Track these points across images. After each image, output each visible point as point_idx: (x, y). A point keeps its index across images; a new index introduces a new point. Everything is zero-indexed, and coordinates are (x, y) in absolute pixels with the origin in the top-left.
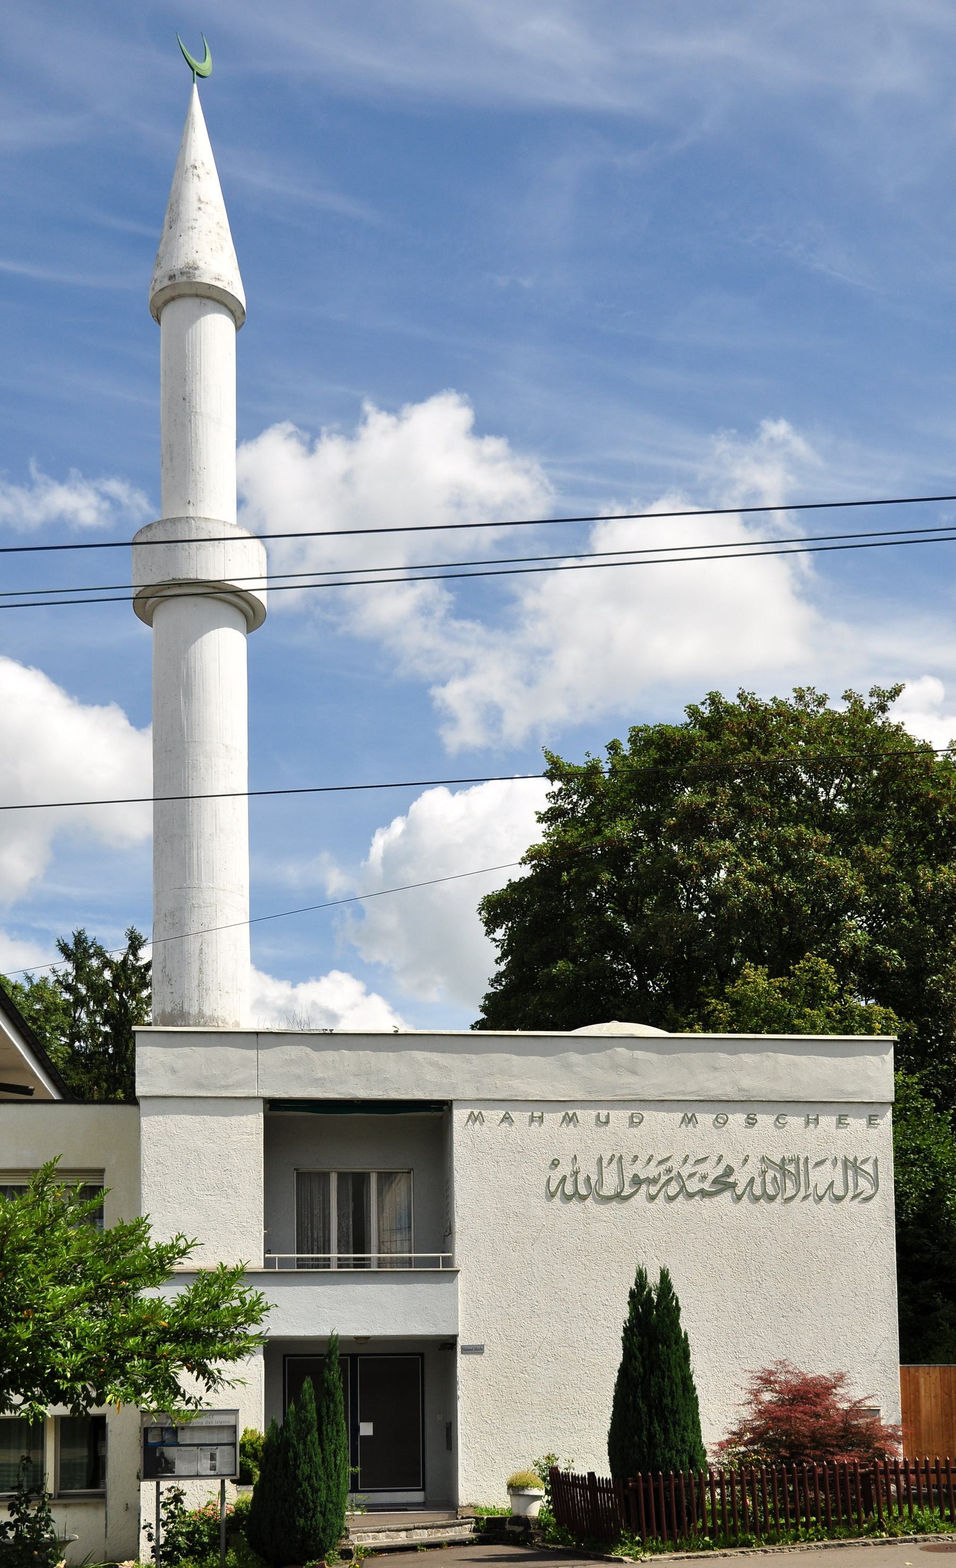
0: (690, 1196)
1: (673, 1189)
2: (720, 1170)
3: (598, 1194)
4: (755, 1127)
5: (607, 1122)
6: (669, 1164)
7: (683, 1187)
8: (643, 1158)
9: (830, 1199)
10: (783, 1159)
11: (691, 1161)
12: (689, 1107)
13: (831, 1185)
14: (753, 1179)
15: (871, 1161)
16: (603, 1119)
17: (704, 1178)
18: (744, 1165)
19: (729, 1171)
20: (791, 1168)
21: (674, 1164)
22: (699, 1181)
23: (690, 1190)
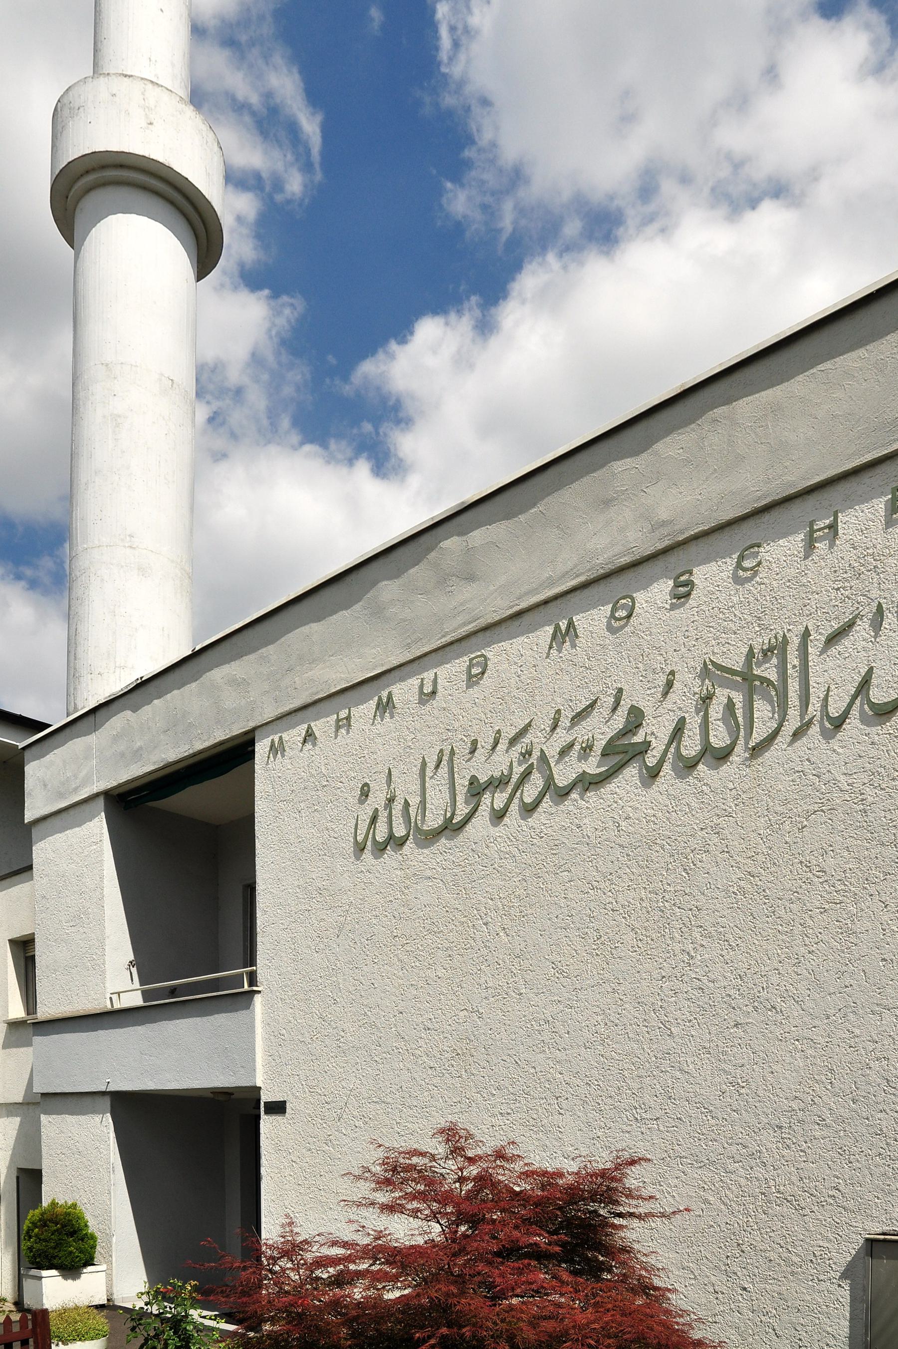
0: (563, 794)
1: (529, 793)
2: (619, 721)
4: (692, 602)
5: (434, 693)
6: (526, 740)
7: (549, 782)
8: (485, 742)
9: (864, 720)
10: (751, 653)
11: (565, 722)
12: (550, 610)
13: (865, 684)
14: (682, 720)
17: (587, 749)
18: (665, 694)
22: (580, 759)
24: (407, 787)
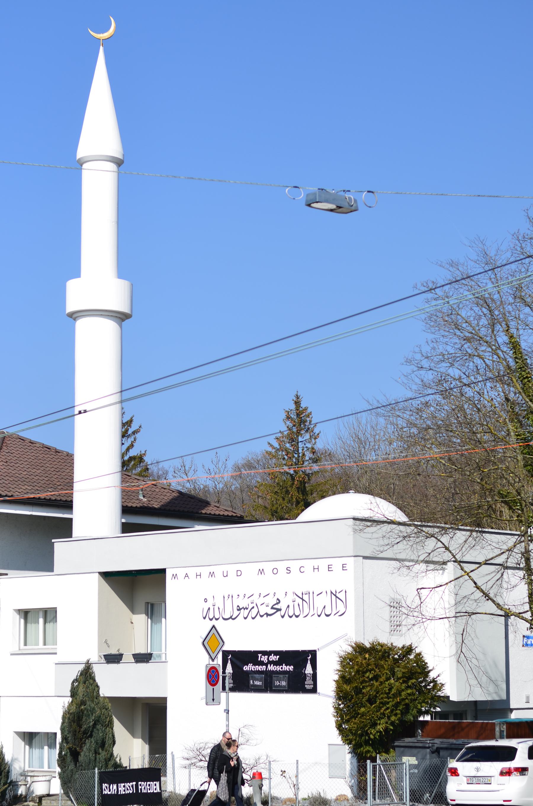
7: (258, 611)
8: (242, 596)
11: (262, 596)
15: (344, 592)
19: (279, 601)
20: (306, 597)
21: (255, 598)
24: (219, 603)
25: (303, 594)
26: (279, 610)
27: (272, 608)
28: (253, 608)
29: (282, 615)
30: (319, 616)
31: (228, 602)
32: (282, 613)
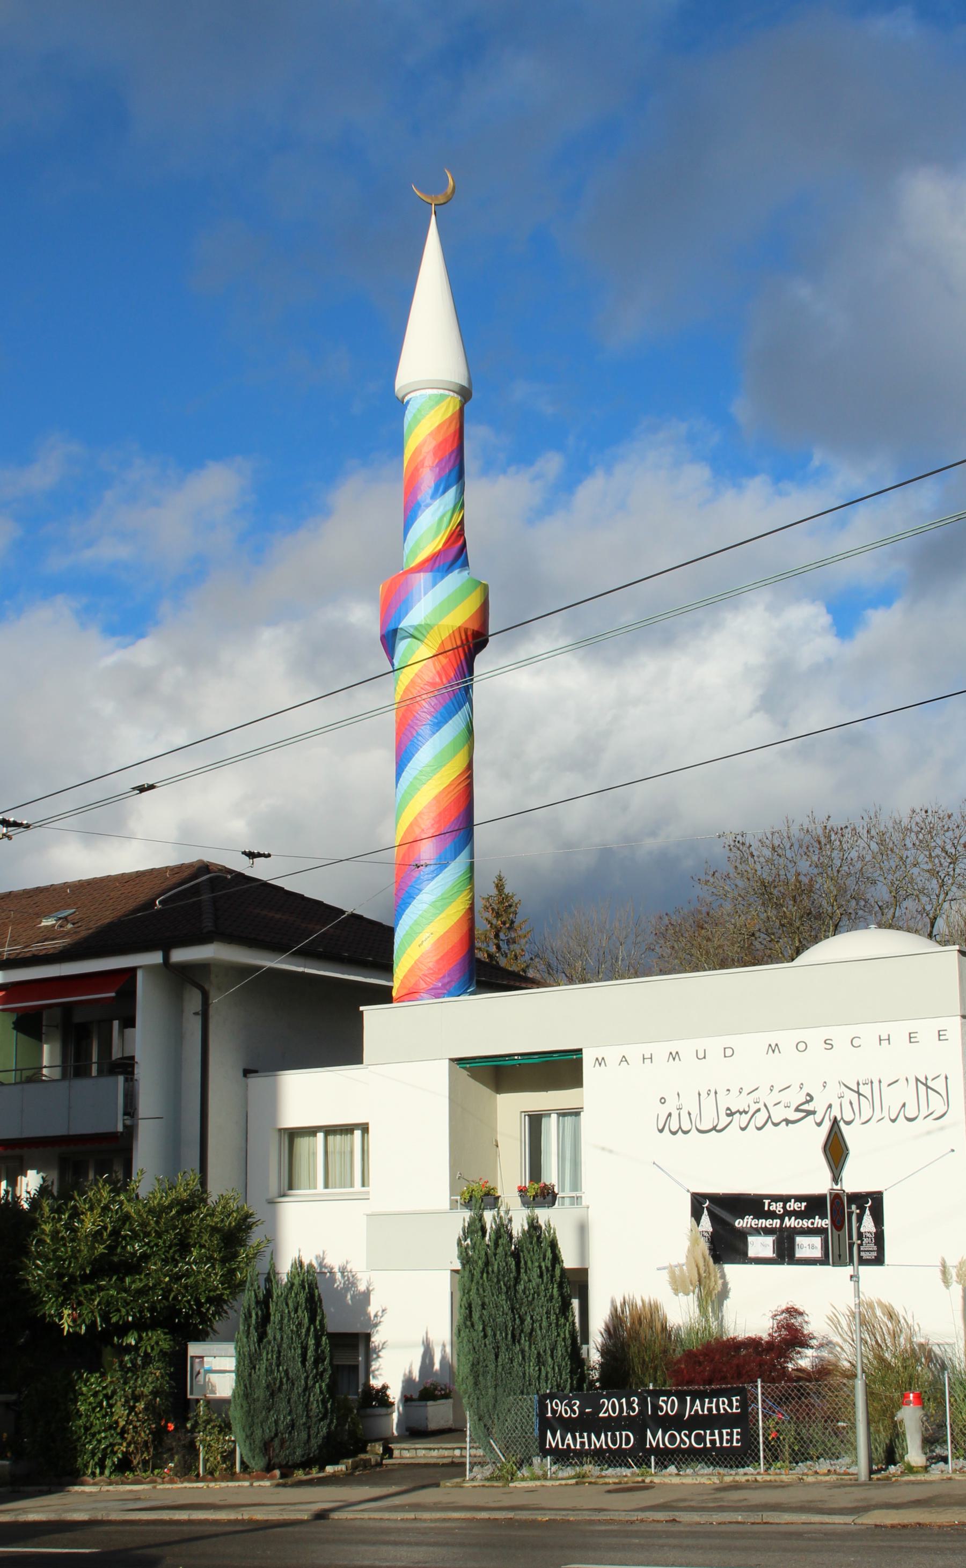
3: (698, 1130)
7: (770, 1117)
8: (735, 1091)
11: (776, 1090)
15: (942, 1078)
16: (701, 1055)
19: (810, 1098)
20: (865, 1090)
23: (776, 1121)
25: (858, 1084)
26: (814, 1113)
27: (797, 1110)
28: (759, 1110)
29: (818, 1121)
30: (893, 1121)
31: (708, 1103)
32: (818, 1118)
